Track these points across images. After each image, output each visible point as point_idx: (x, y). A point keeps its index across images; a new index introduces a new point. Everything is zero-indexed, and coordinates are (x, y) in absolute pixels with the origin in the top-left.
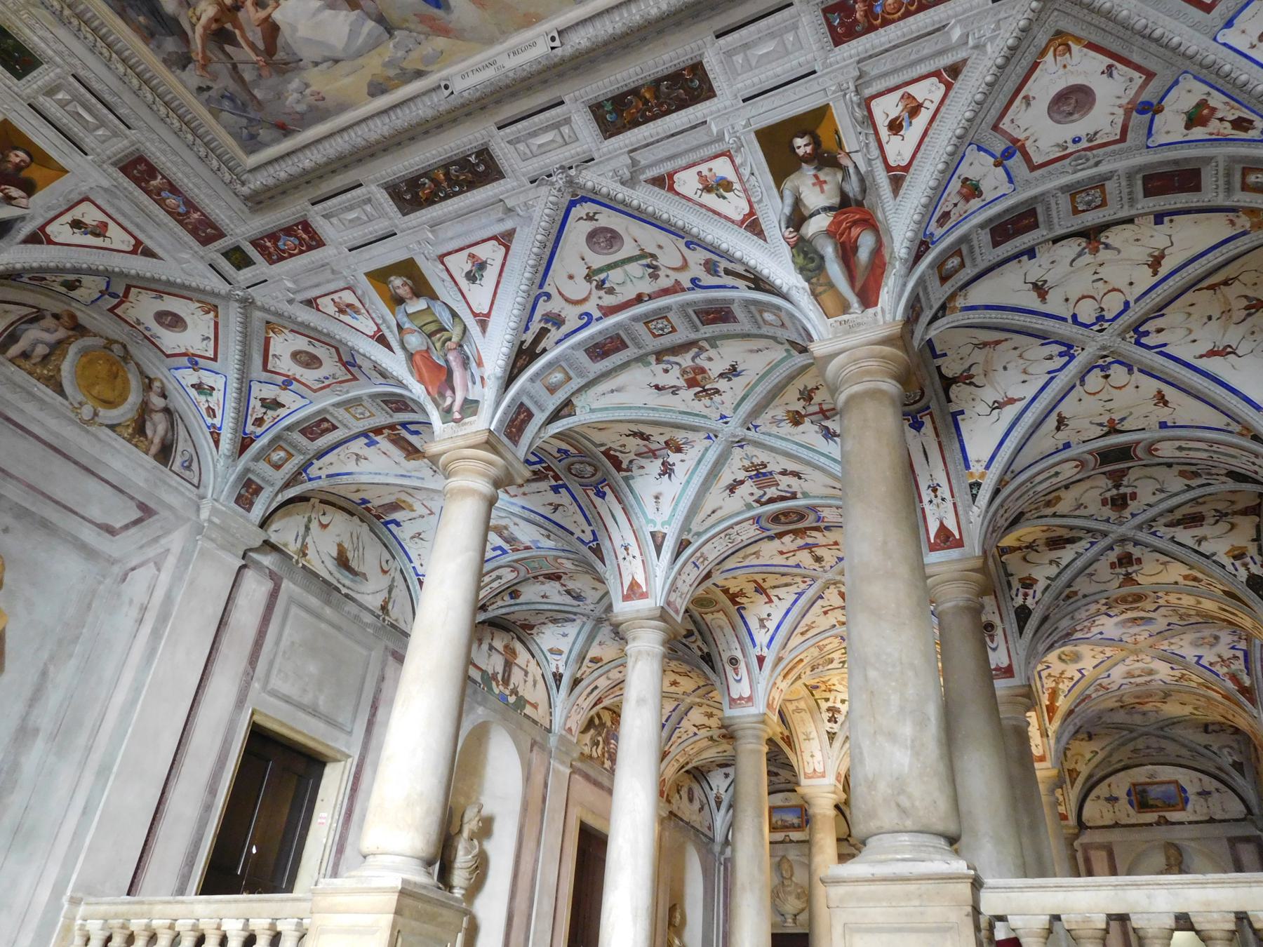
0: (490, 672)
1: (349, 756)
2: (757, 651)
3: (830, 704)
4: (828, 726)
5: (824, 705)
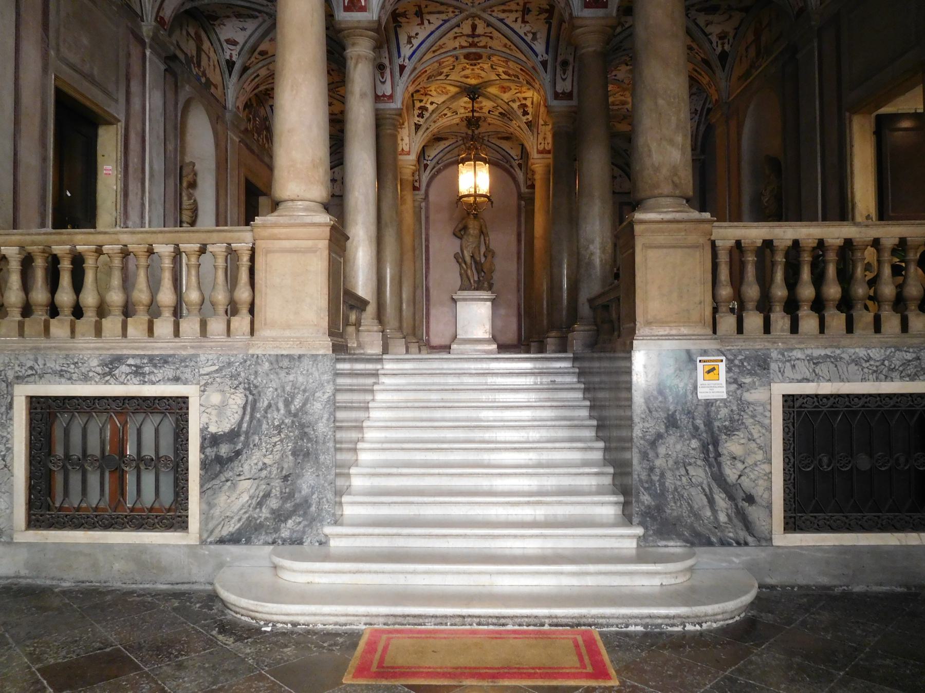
0: (189, 55)
1: (119, 121)
2: (401, 61)
3: (422, 104)
4: (416, 119)
5: (418, 105)
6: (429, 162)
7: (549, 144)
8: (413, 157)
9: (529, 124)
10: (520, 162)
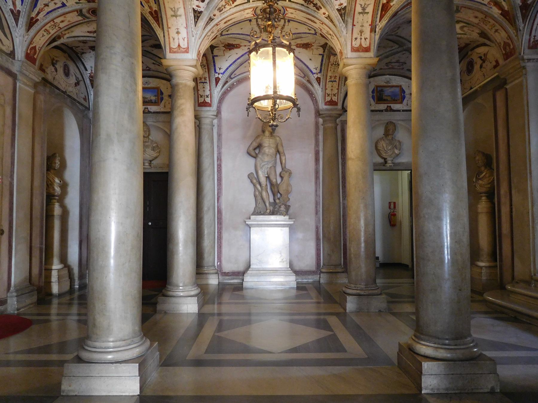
6: (220, 76)
7: (369, 39)
10: (319, 75)
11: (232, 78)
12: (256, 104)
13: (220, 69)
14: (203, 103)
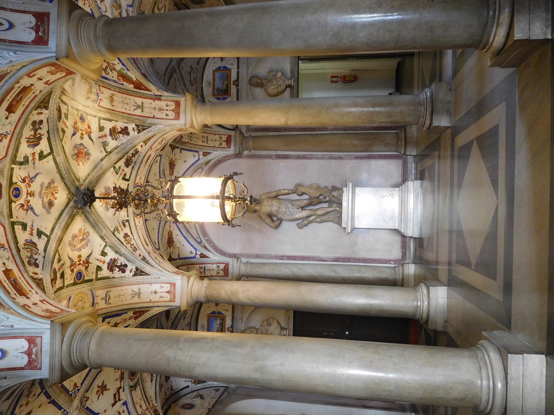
3: (105, 267)
4: (128, 274)
5: (105, 272)
6: (199, 253)
7: (167, 103)
8: (179, 280)
9: (141, 128)
10: (201, 153)
11: (201, 241)
12: (228, 217)
13: (192, 253)
14: (224, 272)
